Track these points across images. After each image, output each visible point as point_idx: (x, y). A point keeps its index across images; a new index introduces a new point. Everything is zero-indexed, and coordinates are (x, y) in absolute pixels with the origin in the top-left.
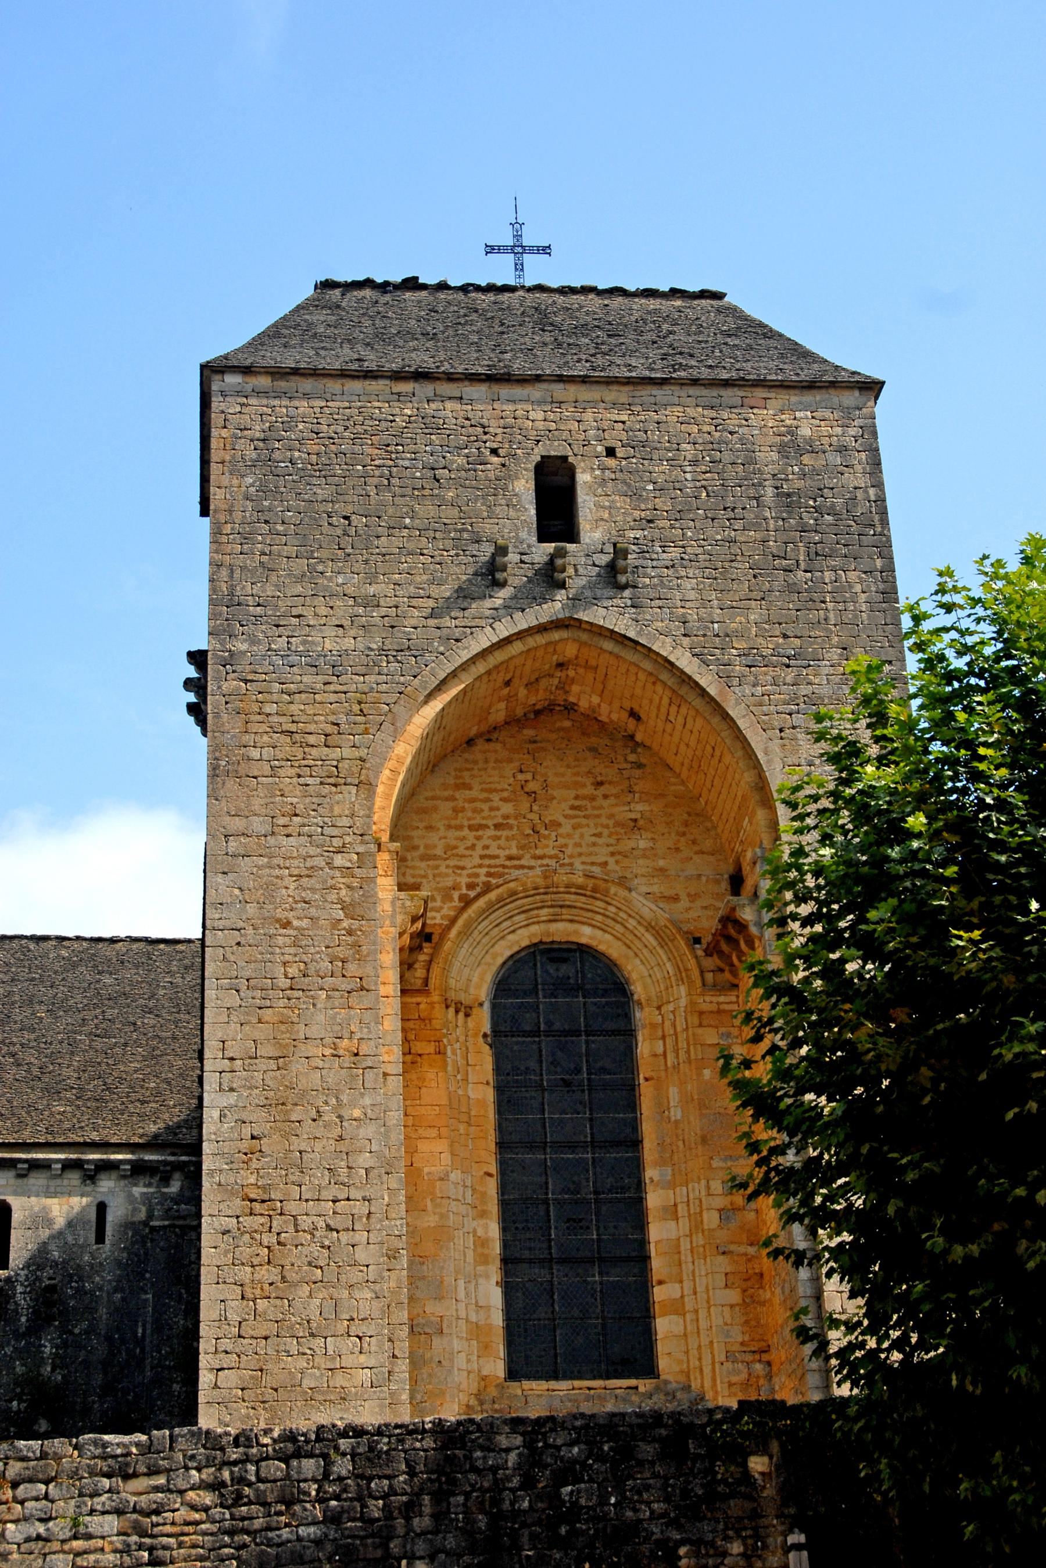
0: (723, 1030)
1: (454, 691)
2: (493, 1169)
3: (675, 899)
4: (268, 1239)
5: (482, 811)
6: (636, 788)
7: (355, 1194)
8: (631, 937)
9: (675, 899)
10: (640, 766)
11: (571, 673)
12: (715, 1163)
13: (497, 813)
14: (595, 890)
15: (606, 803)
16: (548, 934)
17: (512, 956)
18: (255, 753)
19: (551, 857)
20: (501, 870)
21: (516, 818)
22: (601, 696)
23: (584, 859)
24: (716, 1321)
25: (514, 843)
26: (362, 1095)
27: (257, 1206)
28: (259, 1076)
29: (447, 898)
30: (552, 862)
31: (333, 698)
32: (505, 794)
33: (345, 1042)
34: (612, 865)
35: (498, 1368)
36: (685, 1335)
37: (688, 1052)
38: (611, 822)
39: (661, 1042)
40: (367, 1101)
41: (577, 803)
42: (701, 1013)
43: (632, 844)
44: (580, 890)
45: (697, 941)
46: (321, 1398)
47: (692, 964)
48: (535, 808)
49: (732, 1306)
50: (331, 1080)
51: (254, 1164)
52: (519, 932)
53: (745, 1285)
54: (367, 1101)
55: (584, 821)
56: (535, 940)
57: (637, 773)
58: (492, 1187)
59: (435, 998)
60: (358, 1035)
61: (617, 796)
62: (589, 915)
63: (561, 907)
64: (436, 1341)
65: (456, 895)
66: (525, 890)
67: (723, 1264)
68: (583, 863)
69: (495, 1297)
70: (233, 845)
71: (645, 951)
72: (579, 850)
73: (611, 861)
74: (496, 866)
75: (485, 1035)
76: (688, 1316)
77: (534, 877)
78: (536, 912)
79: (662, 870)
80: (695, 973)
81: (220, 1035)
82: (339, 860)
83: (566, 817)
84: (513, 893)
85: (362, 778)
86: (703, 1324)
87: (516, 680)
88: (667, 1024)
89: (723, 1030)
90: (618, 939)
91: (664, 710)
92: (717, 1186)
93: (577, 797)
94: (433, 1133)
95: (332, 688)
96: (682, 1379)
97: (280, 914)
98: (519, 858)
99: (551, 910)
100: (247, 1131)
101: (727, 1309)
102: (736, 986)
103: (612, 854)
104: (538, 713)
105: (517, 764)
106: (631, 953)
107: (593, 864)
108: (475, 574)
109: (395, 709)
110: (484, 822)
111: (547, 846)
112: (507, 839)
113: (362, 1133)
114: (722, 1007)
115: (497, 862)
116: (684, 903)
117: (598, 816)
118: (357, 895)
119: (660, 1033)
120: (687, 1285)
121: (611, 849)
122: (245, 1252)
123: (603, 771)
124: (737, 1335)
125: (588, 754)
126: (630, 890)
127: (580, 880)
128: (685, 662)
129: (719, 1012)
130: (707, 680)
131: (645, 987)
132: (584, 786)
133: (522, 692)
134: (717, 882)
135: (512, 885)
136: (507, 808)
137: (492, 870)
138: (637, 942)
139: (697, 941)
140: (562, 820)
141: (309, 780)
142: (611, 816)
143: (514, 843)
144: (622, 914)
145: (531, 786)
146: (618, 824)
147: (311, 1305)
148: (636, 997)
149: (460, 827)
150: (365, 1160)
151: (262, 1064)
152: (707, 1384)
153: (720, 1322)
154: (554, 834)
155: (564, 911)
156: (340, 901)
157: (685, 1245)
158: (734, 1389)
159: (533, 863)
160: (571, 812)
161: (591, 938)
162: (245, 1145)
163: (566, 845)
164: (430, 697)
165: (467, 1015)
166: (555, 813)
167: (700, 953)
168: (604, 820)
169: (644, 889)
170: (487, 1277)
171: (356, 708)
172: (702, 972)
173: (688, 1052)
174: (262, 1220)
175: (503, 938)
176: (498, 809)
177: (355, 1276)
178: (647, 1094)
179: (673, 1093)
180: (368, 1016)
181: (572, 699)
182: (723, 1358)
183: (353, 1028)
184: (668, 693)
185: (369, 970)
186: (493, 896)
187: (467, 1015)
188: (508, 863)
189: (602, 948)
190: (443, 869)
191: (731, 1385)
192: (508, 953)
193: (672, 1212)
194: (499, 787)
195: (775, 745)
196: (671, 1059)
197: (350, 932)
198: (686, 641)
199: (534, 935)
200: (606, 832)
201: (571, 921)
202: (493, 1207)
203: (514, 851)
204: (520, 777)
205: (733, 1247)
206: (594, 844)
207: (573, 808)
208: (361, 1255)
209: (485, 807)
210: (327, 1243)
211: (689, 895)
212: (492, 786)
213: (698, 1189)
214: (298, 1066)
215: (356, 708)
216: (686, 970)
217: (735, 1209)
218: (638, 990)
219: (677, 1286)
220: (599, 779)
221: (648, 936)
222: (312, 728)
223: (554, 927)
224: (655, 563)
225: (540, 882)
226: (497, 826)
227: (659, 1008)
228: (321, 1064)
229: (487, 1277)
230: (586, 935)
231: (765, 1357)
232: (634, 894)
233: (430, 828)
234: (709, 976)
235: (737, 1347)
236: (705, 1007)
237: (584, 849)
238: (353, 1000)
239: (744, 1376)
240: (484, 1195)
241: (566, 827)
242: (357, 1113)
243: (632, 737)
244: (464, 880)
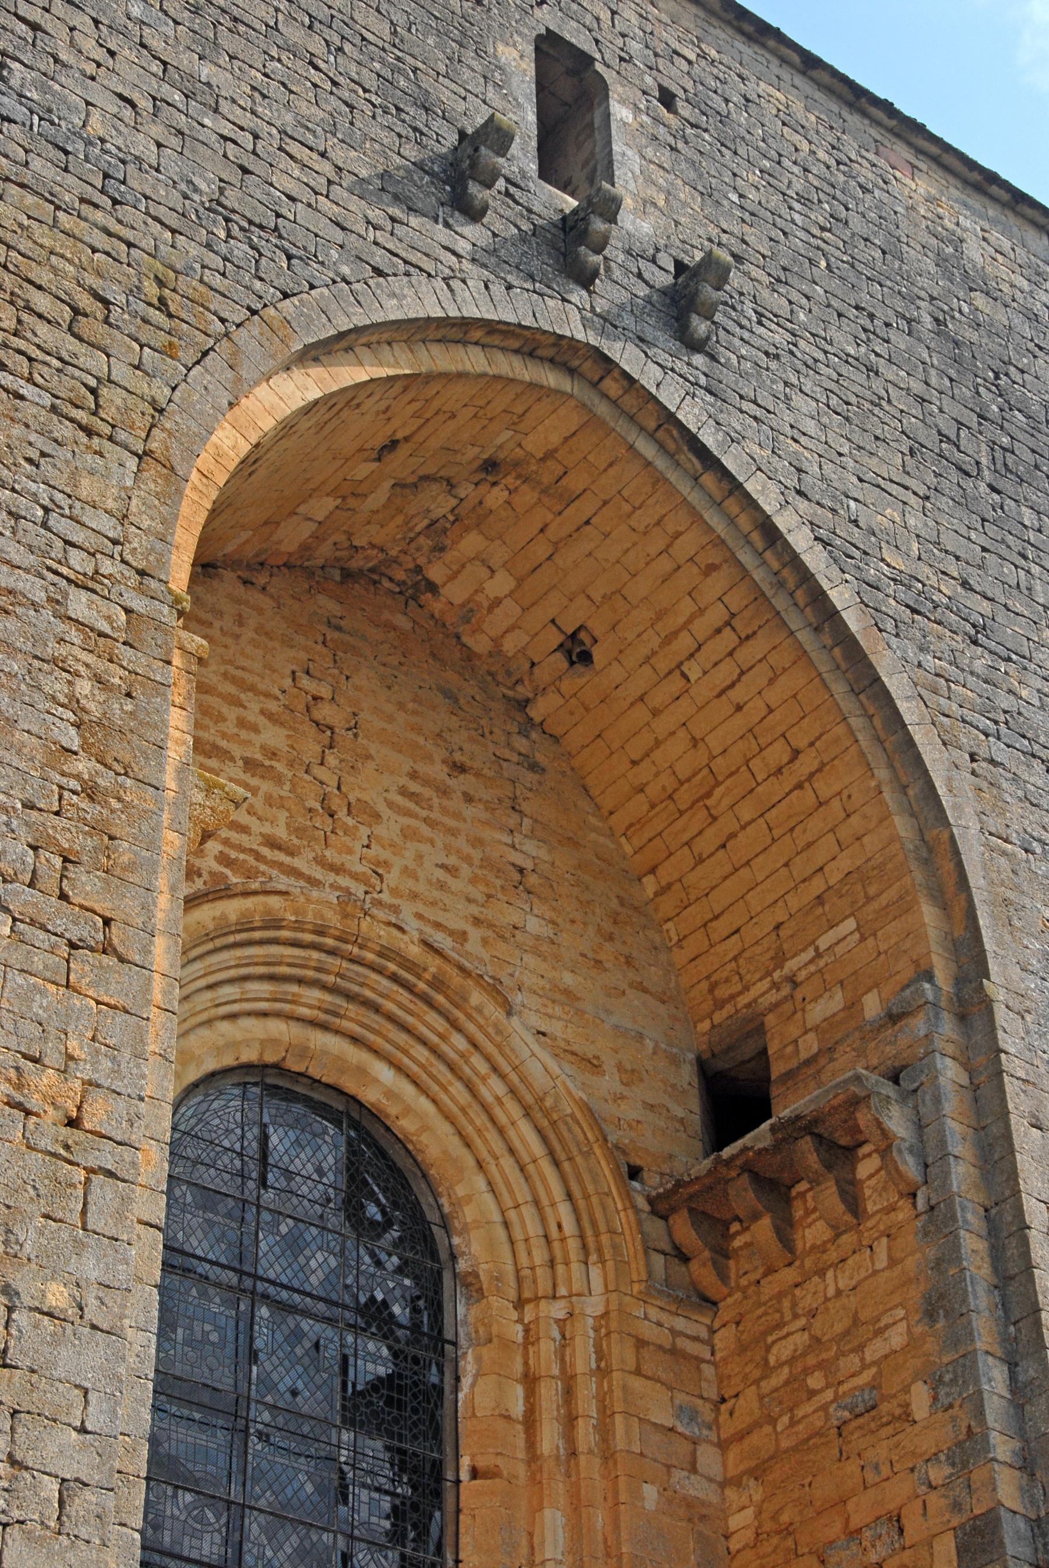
0: (681, 1398)
1: (350, 374)
3: (594, 1065)
5: (221, 718)
6: (525, 807)
8: (481, 1120)
11: (496, 497)
13: (253, 736)
14: (438, 983)
15: (469, 811)
16: (304, 1052)
19: (355, 876)
20: (251, 860)
21: (291, 765)
22: (520, 581)
23: (421, 908)
25: (282, 816)
26: (79, 1246)
30: (359, 890)
31: (99, 240)
32: (273, 706)
34: (473, 945)
38: (477, 855)
39: (519, 1390)
41: (414, 787)
42: (641, 1343)
43: (513, 916)
45: (634, 1173)
48: (331, 760)
52: (245, 1022)
54: (90, 1268)
55: (425, 830)
56: (270, 1058)
57: (531, 777)
60: (84, 1071)
61: (489, 807)
62: (402, 1038)
63: (349, 997)
66: (298, 926)
68: (419, 916)
71: (507, 1163)
72: (410, 883)
73: (475, 934)
74: (244, 850)
77: (321, 905)
78: (294, 988)
79: (567, 992)
82: (79, 604)
83: (390, 805)
84: (275, 924)
85: (153, 445)
88: (547, 1348)
89: (681, 1398)
90: (448, 1117)
91: (685, 642)
93: (413, 775)
95: (99, 216)
98: (291, 854)
99: (328, 997)
102: (709, 1302)
103: (477, 921)
104: (348, 575)
105: (303, 656)
106: (471, 1162)
107: (438, 925)
108: (419, 165)
109: (241, 336)
110: (223, 744)
111: (350, 851)
112: (269, 800)
114: (682, 1343)
115: (244, 840)
116: (609, 1082)
117: (453, 832)
118: (119, 709)
119: (518, 1367)
121: (475, 910)
123: (467, 746)
125: (439, 699)
126: (509, 1013)
127: (414, 951)
129: (674, 1352)
131: (491, 1246)
132: (429, 758)
134: (675, 1061)
135: (274, 901)
136: (274, 736)
137: (233, 854)
138: (492, 1136)
139: (634, 1173)
140: (382, 808)
141: (28, 390)
142: (477, 842)
143: (282, 816)
144: (476, 1060)
145: (325, 712)
146: (486, 863)
148: (462, 1265)
150: (59, 1451)
154: (364, 831)
155: (353, 1010)
156: (73, 703)
159: (318, 873)
160: (399, 799)
161: (390, 1094)
163: (386, 864)
164: (314, 354)
166: (370, 787)
167: (641, 1203)
168: (461, 843)
169: (537, 1022)
171: (151, 290)
175: (209, 1022)
176: (255, 729)
180: (116, 1027)
181: (436, 573)
183: (73, 1044)
184: (736, 600)
186: (232, 909)
188: (265, 851)
189: (406, 1125)
194: (262, 687)
195: (965, 781)
196: (550, 1438)
199: (274, 1042)
200: (465, 871)
201: (355, 1040)
203: (281, 832)
204: (305, 682)
206: (442, 886)
207: (403, 792)
209: (231, 713)
211: (620, 1067)
212: (251, 679)
216: (611, 1231)
220: (458, 757)
221: (525, 1127)
222: (44, 277)
223: (320, 1039)
224: (746, 335)
225: (333, 919)
226: (249, 764)
232: (515, 1021)
236: (648, 1331)
237: (421, 888)
238: (84, 966)
241: (390, 827)
242: (57, 1296)
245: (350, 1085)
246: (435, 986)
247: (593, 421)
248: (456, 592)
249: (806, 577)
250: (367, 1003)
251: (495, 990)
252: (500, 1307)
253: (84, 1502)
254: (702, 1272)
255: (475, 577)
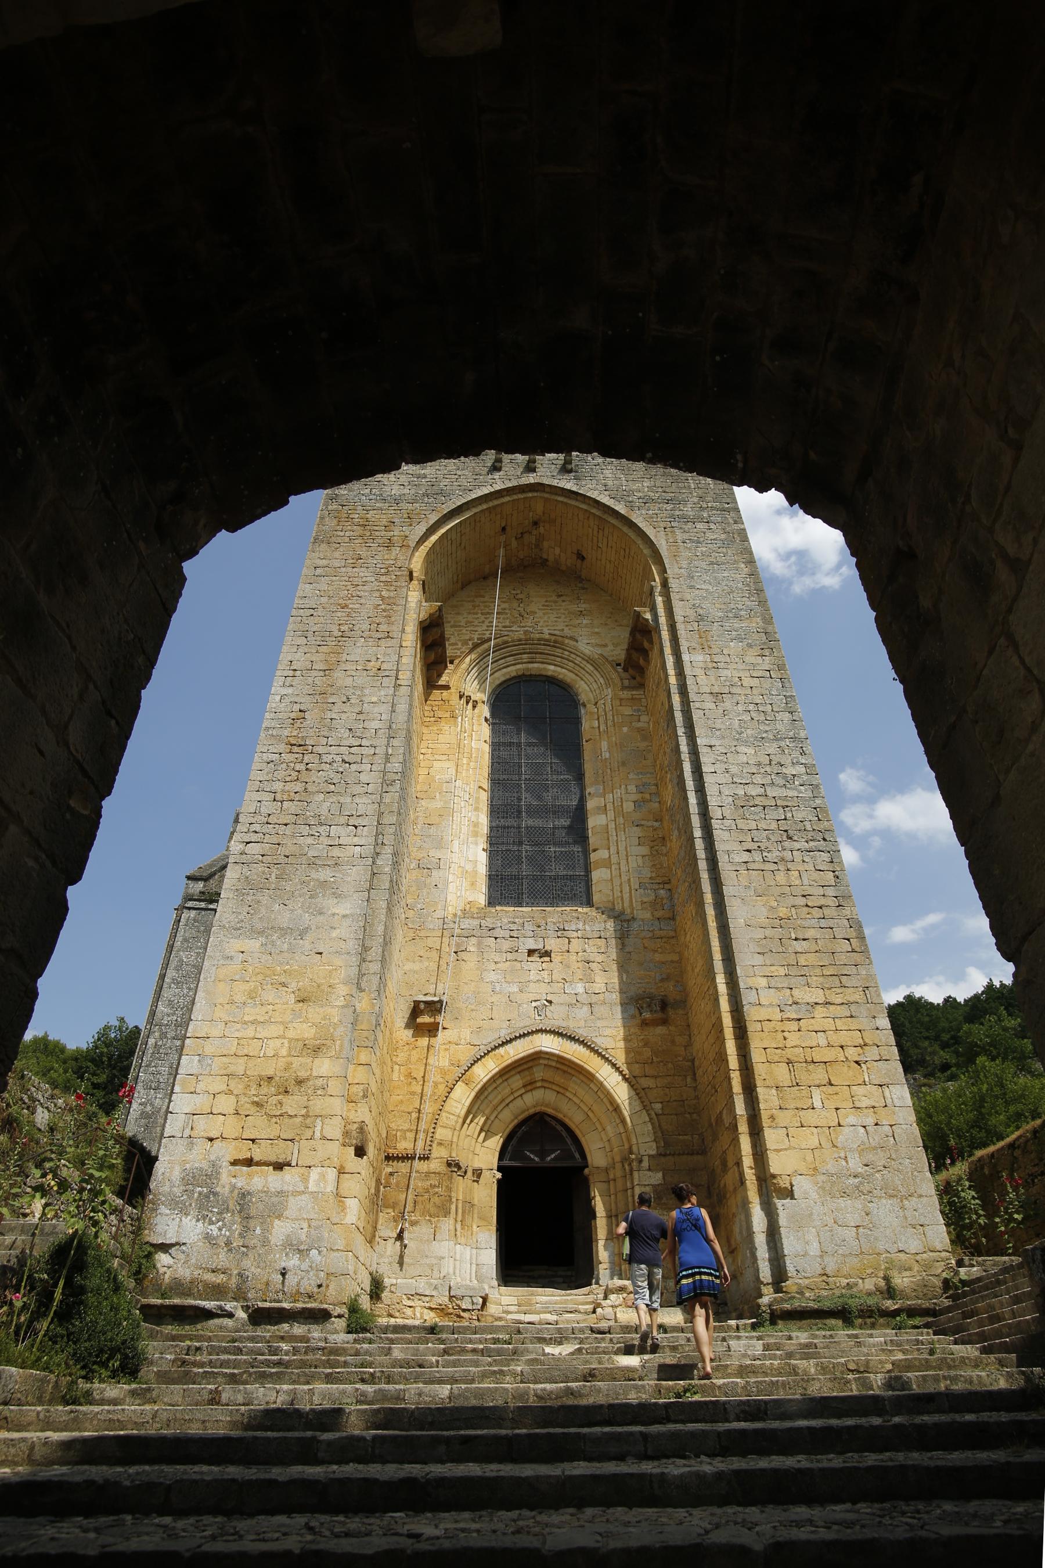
2: (485, 787)
4: (301, 767)
7: (364, 742)
8: (578, 668)
9: (605, 646)
10: (583, 588)
12: (631, 776)
14: (555, 642)
16: (528, 669)
17: (505, 681)
18: (342, 534)
24: (633, 864)
26: (379, 690)
27: (296, 749)
28: (310, 680)
29: (465, 643)
33: (372, 664)
35: (482, 899)
36: (611, 880)
37: (613, 720)
40: (382, 693)
42: (621, 700)
44: (546, 643)
46: (321, 863)
47: (614, 676)
49: (643, 856)
50: (359, 681)
51: (298, 724)
53: (652, 844)
54: (382, 693)
56: (520, 673)
58: (484, 796)
59: (453, 690)
64: (435, 873)
65: (470, 643)
66: (513, 641)
67: (637, 831)
69: (483, 858)
70: (319, 571)
71: (587, 675)
73: (566, 629)
75: (486, 720)
76: (613, 867)
77: (520, 634)
79: (597, 633)
80: (617, 681)
81: (290, 659)
82: (383, 578)
84: (506, 642)
86: (623, 868)
87: (508, 529)
92: (632, 788)
94: (445, 757)
96: (610, 906)
97: (341, 601)
100: (296, 707)
101: (640, 859)
104: (525, 567)
113: (376, 710)
116: (610, 647)
120: (613, 849)
122: (280, 774)
124: (647, 873)
127: (547, 637)
128: (605, 500)
130: (621, 508)
133: (514, 544)
145: (519, 596)
147: (322, 805)
149: (477, 614)
151: (314, 673)
152: (627, 904)
153: (635, 865)
156: (381, 596)
157: (612, 826)
158: (644, 906)
162: (293, 715)
165: (474, 707)
166: (533, 607)
168: (562, 611)
170: (477, 844)
172: (621, 679)
173: (613, 720)
174: (297, 756)
177: (358, 789)
178: (587, 748)
179: (604, 745)
181: (545, 556)
182: (637, 887)
185: (394, 628)
187: (474, 707)
189: (561, 677)
190: (464, 631)
191: (643, 903)
192: (503, 679)
193: (604, 810)
197: (384, 611)
198: (606, 493)
201: (542, 663)
202: (484, 807)
203: (508, 624)
205: (643, 822)
208: (364, 778)
210: (341, 770)
213: (618, 793)
214: (338, 674)
215: (406, 516)
217: (644, 801)
218: (582, 698)
219: (606, 851)
223: (531, 666)
225: (523, 637)
227: (596, 704)
228: (354, 674)
229: (477, 844)
230: (551, 669)
231: (667, 886)
233: (458, 614)
234: (626, 683)
235: (647, 880)
236: (623, 696)
238: (382, 642)
239: (652, 897)
240: (478, 798)
241: (540, 613)
242: (374, 699)
243: (580, 577)
244: (476, 637)
245: (544, 673)
246: (555, 643)
247: (546, 500)
248: (551, 558)
249: (609, 507)
250: (541, 653)
251: (572, 638)
252: (591, 707)
253: (380, 732)
254: (638, 678)
255: (553, 552)
